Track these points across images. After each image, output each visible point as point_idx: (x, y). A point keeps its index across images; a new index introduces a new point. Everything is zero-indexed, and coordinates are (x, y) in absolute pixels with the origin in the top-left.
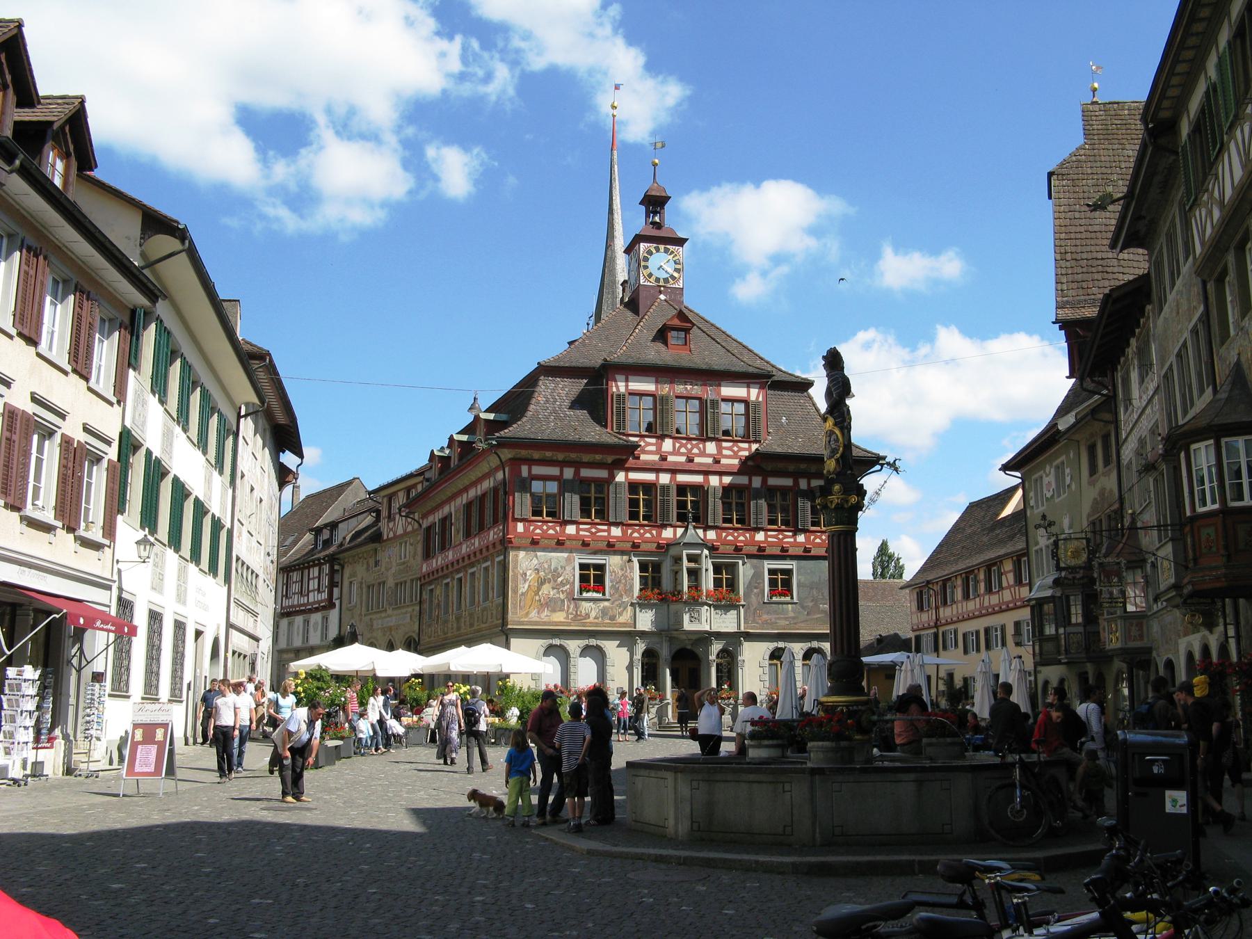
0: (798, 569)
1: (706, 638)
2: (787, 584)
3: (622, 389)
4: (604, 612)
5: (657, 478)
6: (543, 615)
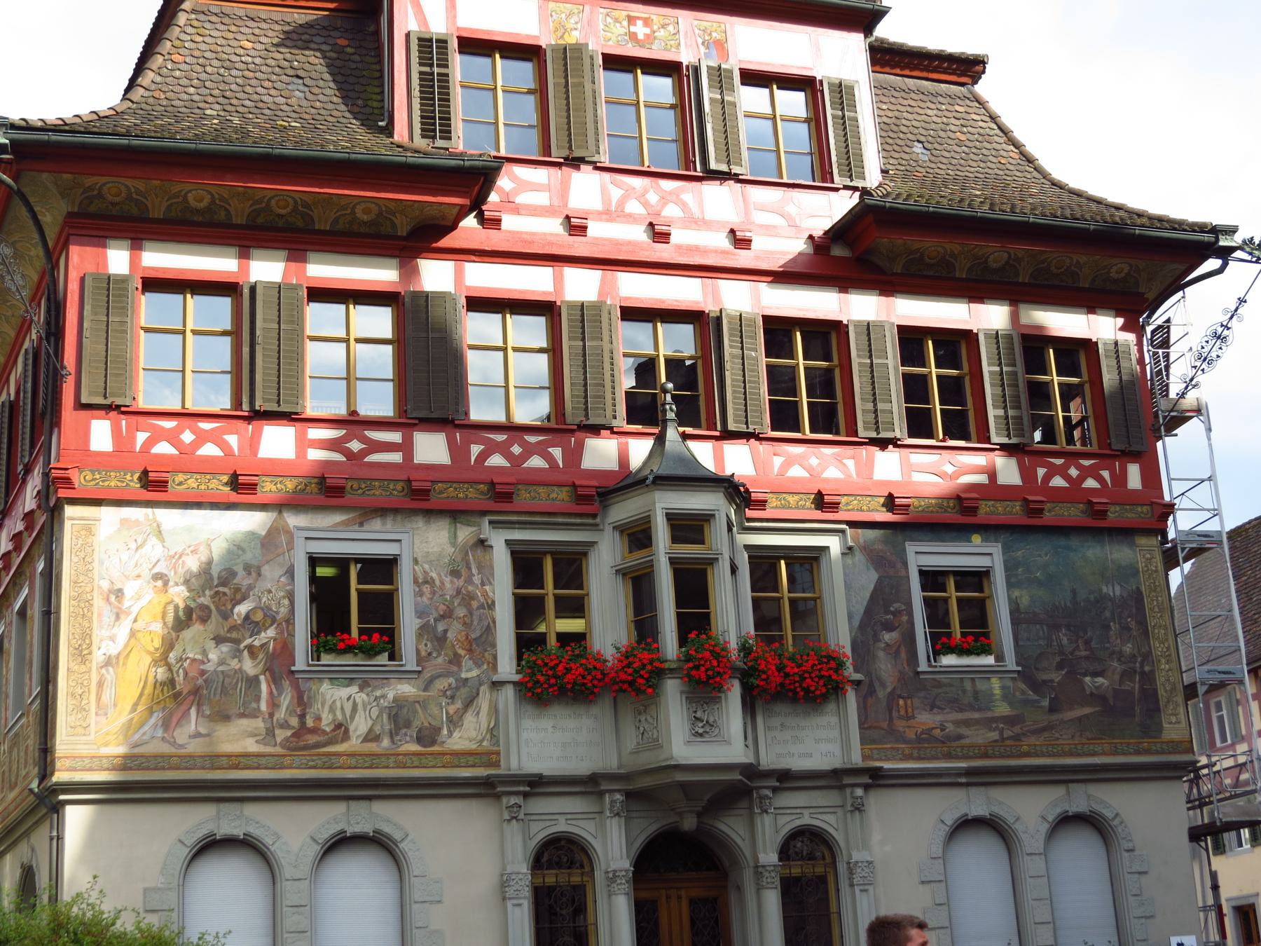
0: (1010, 568)
1: (744, 787)
2: (977, 616)
3: (438, 26)
4: (399, 716)
5: (558, 281)
6: (183, 735)
